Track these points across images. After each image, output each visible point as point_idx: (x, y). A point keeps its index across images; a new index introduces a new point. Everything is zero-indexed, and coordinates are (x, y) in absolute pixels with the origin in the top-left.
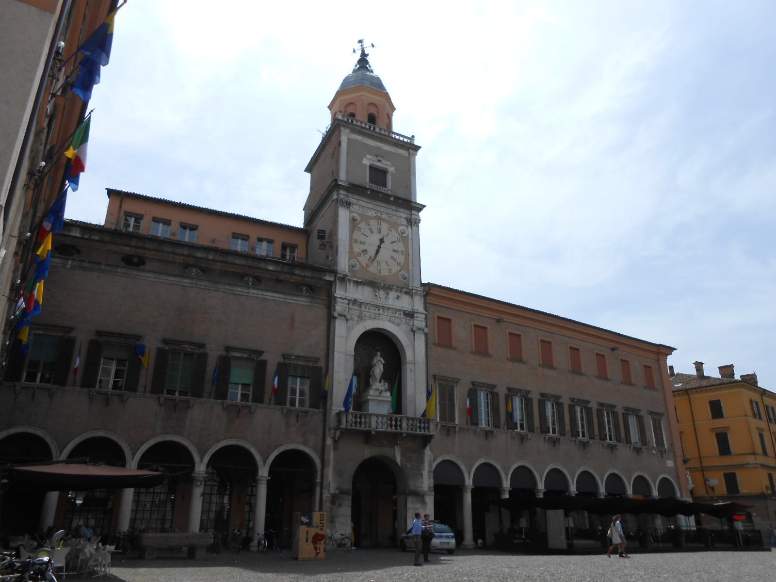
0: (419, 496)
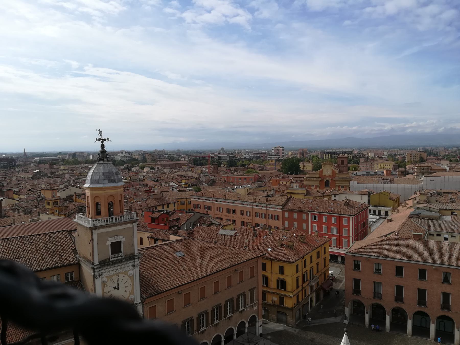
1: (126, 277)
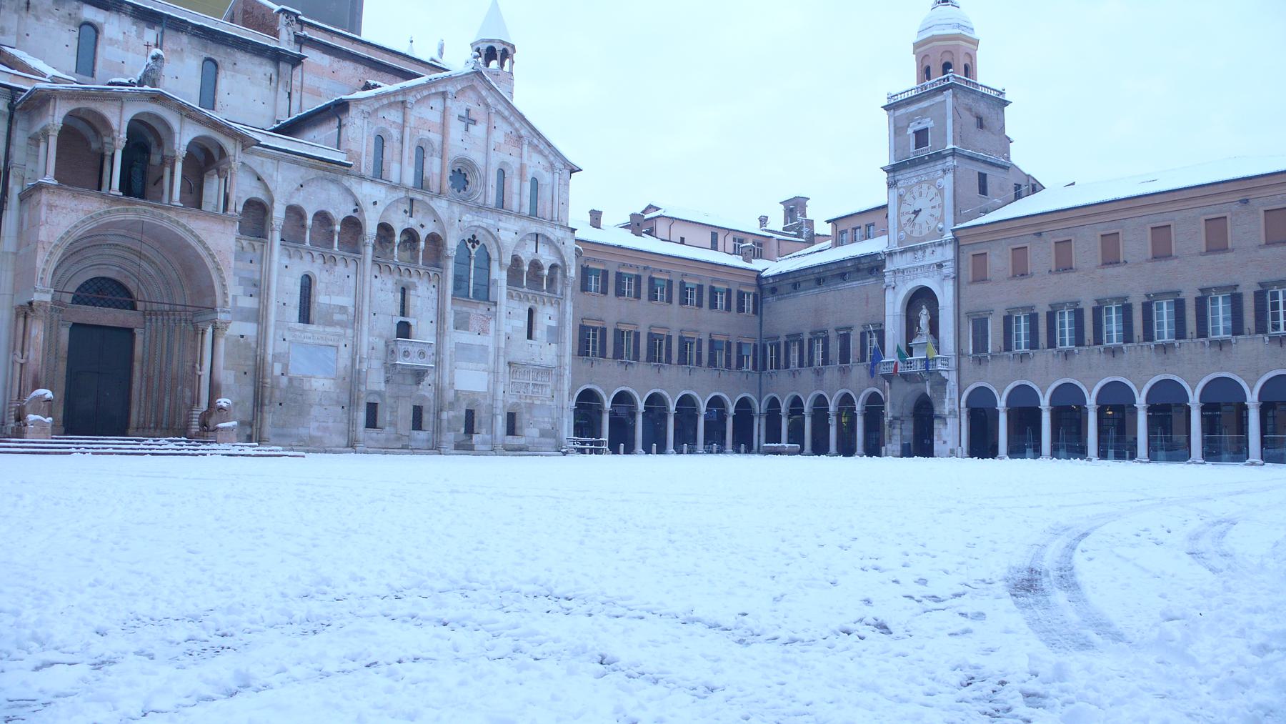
0: (943, 419)
1: (933, 190)
